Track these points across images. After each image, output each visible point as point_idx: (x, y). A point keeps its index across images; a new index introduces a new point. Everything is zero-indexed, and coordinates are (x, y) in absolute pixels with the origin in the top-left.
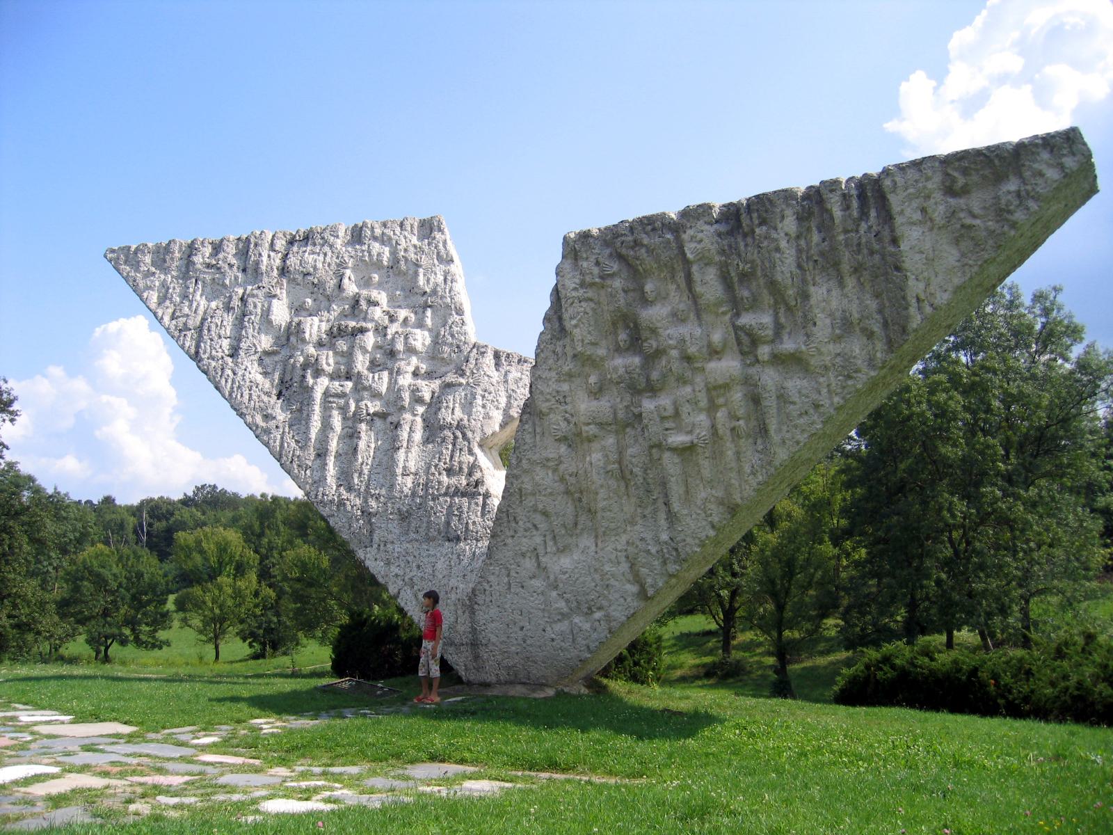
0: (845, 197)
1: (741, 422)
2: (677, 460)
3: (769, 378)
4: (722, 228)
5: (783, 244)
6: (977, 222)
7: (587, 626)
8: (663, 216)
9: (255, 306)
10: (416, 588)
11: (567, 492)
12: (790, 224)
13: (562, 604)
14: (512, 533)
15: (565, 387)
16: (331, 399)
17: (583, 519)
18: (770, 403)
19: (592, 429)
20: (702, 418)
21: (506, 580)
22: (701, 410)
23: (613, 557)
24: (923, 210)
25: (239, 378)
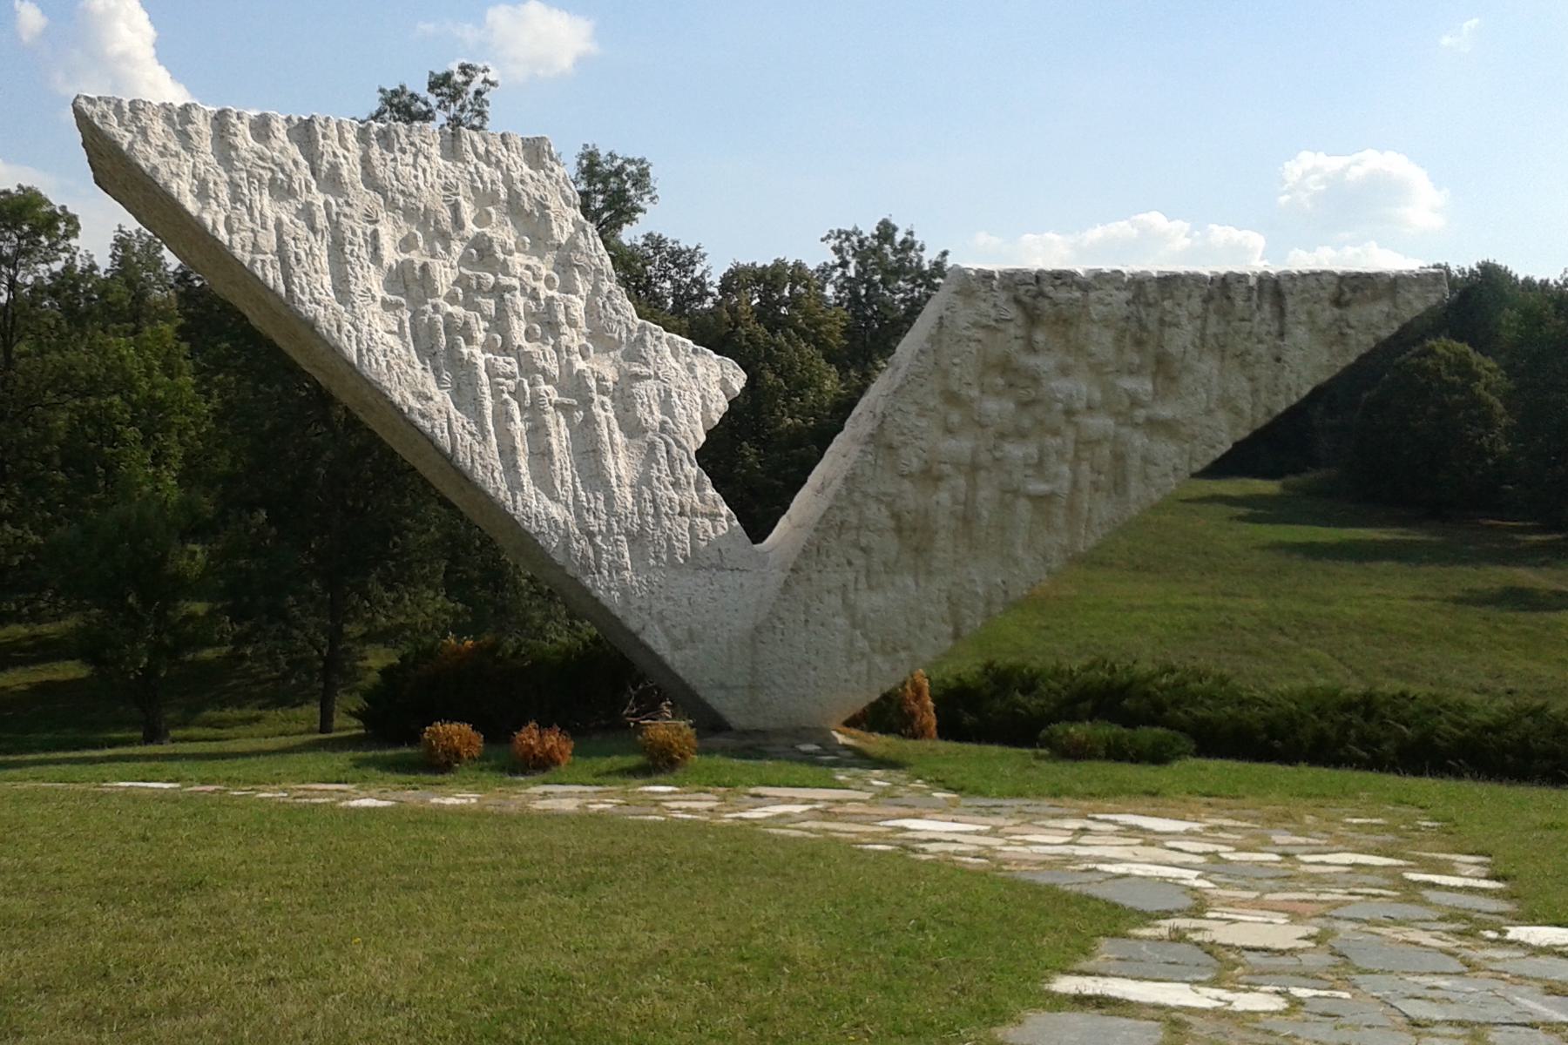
0: (1250, 289)
1: (1102, 478)
3: (1138, 440)
4: (1127, 295)
5: (1184, 321)
8: (1073, 274)
9: (354, 233)
10: (668, 623)
11: (899, 530)
12: (1196, 305)
13: (862, 644)
14: (820, 567)
16: (501, 380)
18: (1135, 462)
19: (947, 468)
20: (1065, 469)
21: (803, 617)
24: (1310, 313)
25: (365, 336)
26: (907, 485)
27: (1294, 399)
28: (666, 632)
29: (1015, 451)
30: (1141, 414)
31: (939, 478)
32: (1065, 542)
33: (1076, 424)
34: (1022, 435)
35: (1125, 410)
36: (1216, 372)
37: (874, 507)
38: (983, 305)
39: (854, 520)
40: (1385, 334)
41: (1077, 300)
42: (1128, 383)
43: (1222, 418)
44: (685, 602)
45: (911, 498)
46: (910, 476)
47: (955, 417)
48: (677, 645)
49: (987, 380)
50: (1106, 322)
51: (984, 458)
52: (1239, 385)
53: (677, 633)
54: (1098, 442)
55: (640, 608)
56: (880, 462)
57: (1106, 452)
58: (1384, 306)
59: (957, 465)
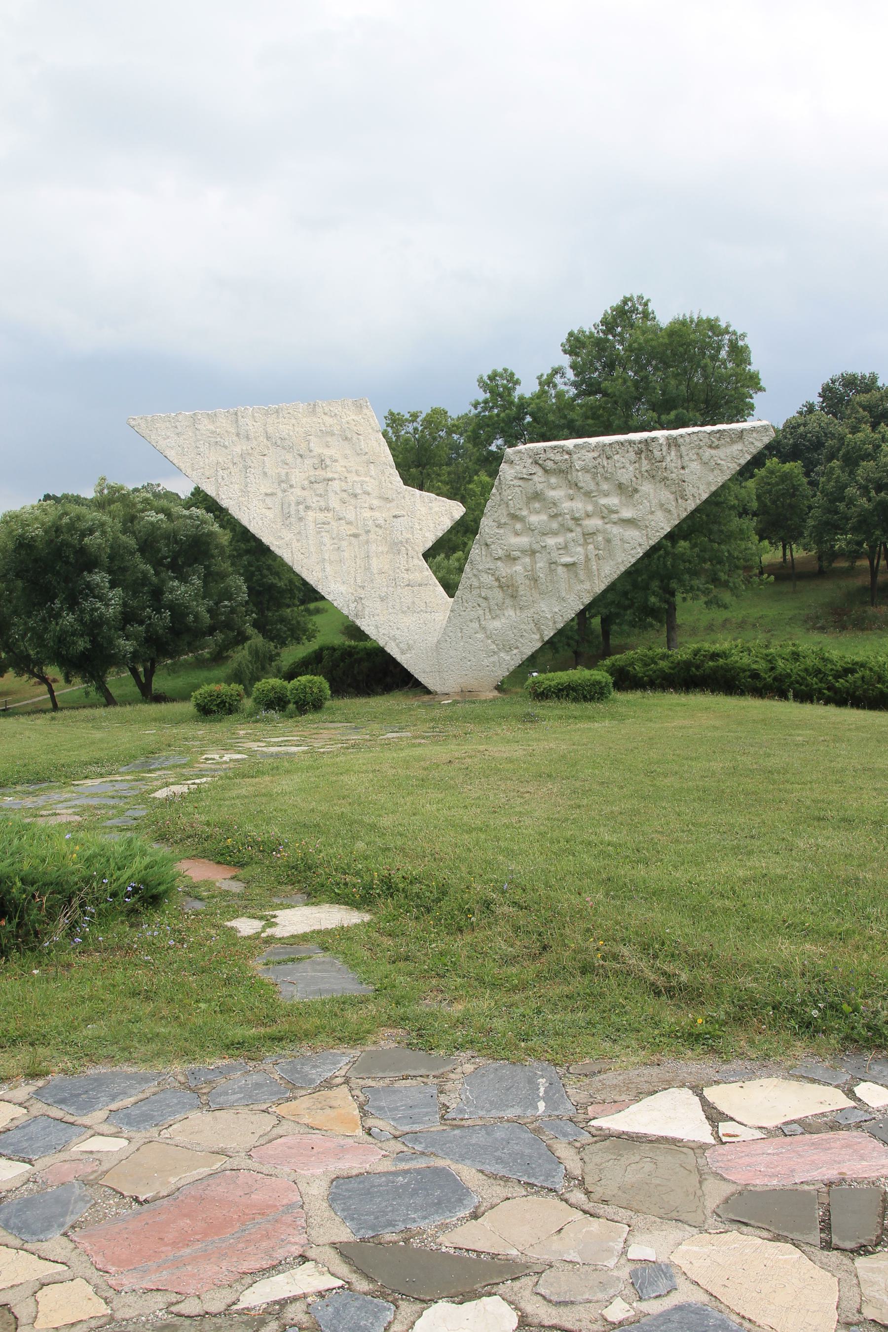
0: (661, 445)
2: (565, 570)
3: (616, 530)
6: (722, 462)
7: (508, 658)
11: (500, 587)
15: (501, 531)
17: (508, 601)
18: (616, 542)
19: (517, 554)
22: (580, 545)
23: (526, 621)
24: (698, 454)
26: (499, 563)
27: (698, 502)
28: (397, 645)
29: (551, 541)
30: (614, 517)
31: (515, 559)
32: (589, 588)
33: (580, 525)
34: (555, 533)
35: (606, 514)
36: (651, 490)
37: (485, 576)
38: (518, 467)
39: (476, 584)
40: (743, 462)
41: (566, 460)
42: (603, 501)
43: (659, 514)
44: (406, 630)
45: (504, 570)
46: (499, 559)
47: (518, 526)
48: (403, 652)
49: (531, 506)
50: (585, 469)
51: (536, 547)
52: (666, 495)
53: (401, 645)
54: (594, 533)
55: (384, 634)
56: (484, 553)
57: (600, 539)
58: (738, 446)
59: (523, 552)
